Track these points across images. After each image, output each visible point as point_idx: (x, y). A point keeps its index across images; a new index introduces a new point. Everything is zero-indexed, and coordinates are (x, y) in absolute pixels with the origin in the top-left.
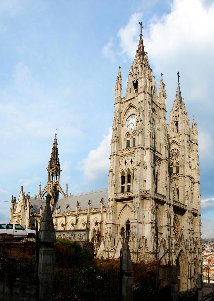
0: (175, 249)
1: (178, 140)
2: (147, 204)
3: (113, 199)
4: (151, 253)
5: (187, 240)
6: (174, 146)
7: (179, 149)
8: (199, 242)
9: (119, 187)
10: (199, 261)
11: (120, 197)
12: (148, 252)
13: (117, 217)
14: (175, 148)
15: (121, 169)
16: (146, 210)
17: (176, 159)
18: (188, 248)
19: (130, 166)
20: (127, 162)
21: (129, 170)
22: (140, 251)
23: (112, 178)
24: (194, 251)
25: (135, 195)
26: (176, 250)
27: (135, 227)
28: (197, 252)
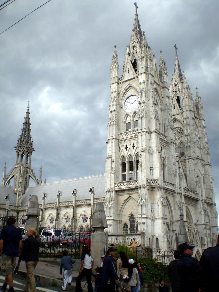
2: (156, 195)
6: (176, 124)
11: (121, 187)
14: (177, 126)
15: (122, 155)
19: (133, 152)
20: (128, 146)
21: (130, 155)
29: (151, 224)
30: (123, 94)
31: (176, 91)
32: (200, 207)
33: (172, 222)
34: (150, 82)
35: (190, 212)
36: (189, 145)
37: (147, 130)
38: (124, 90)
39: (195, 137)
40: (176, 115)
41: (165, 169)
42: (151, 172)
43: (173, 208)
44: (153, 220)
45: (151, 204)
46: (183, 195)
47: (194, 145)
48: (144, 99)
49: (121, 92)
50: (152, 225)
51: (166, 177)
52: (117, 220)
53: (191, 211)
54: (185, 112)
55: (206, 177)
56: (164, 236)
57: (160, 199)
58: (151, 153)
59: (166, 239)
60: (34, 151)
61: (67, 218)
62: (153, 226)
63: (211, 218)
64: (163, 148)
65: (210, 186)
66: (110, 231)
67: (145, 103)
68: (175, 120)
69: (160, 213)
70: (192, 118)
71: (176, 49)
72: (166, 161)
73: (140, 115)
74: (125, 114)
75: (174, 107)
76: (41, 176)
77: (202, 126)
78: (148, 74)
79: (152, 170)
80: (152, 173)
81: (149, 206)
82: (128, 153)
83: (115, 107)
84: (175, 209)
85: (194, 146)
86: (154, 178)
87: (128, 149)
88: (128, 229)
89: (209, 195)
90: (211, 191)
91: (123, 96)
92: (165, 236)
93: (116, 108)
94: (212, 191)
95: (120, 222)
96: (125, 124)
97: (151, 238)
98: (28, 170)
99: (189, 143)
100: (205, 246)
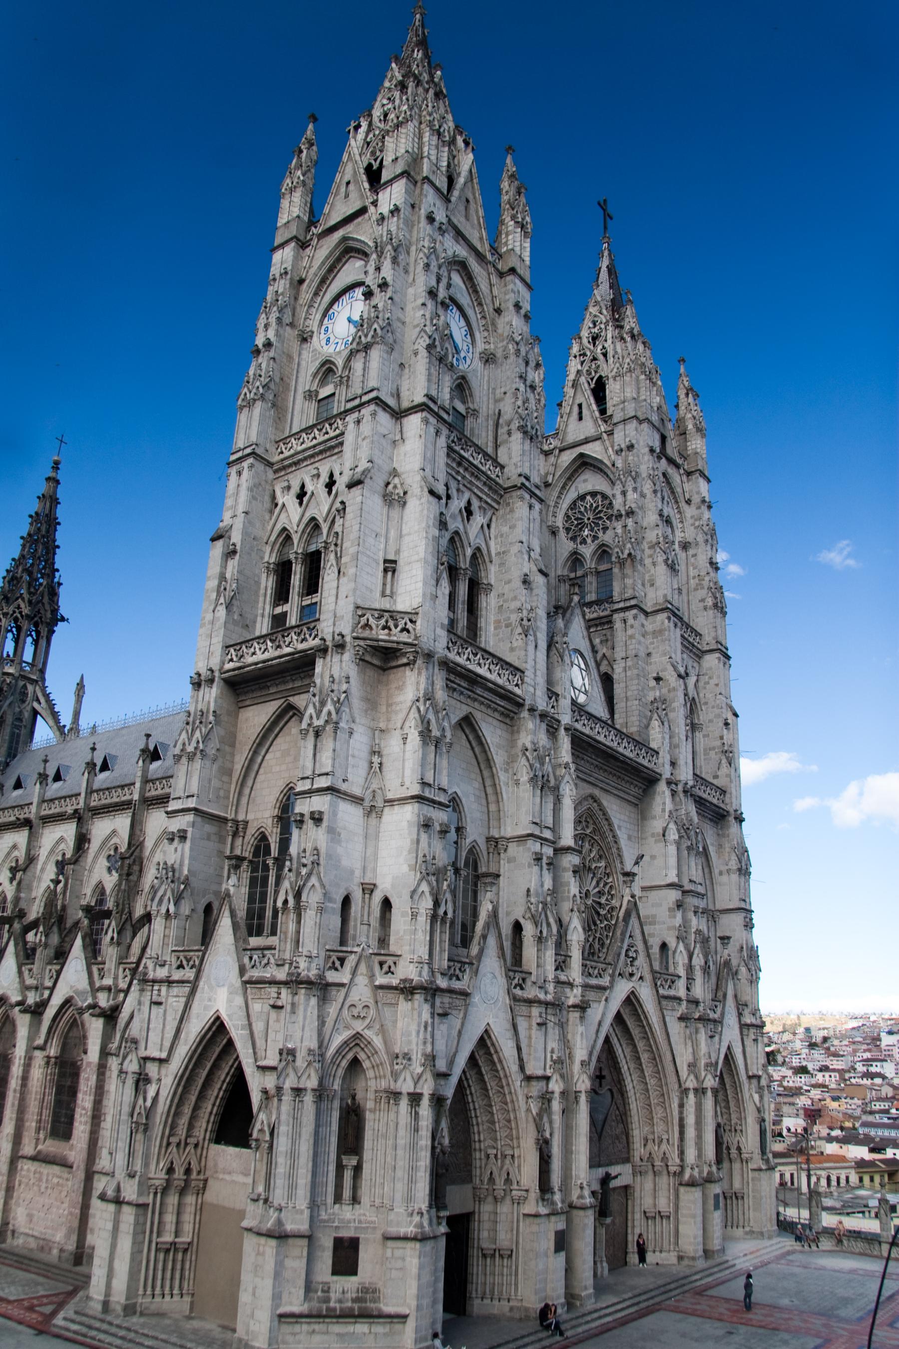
0: (586, 986)
1: (606, 450)
2: (400, 688)
3: (217, 674)
4: (408, 990)
5: (664, 946)
6: (585, 481)
7: (608, 492)
8: (743, 969)
9: (259, 619)
11: (250, 660)
12: (395, 982)
13: (234, 780)
15: (279, 527)
16: (390, 726)
17: (595, 538)
18: (672, 993)
19: (321, 507)
20: (309, 488)
22: (343, 976)
23: (224, 566)
24: (712, 1015)
25: (329, 638)
26: (591, 995)
27: (312, 818)
28: (731, 1020)
29: (360, 831)
30: (315, 284)
31: (595, 359)
32: (663, 810)
33: (495, 844)
35: (610, 825)
36: (630, 555)
37: (391, 402)
38: (320, 268)
39: (660, 523)
40: (587, 441)
41: (484, 604)
42: (384, 584)
43: (502, 777)
44: (373, 808)
45: (373, 730)
46: (566, 729)
47: (650, 556)
48: (387, 271)
52: (226, 820)
53: (616, 822)
54: (621, 426)
55: (706, 703)
56: (419, 885)
57: (414, 709)
59: (427, 903)
60: (63, 619)
61: (112, 853)
62: (371, 837)
64: (480, 507)
65: (722, 738)
66: (176, 866)
67: (390, 289)
68: (584, 463)
69: (408, 772)
70: (647, 450)
71: (607, 216)
72: (493, 569)
73: (363, 338)
74: (317, 364)
75: (580, 413)
76: (77, 715)
77: (696, 499)
78: (419, 184)
79: (390, 574)
80: (388, 586)
81: (356, 736)
82: (303, 516)
83: (271, 334)
84: (517, 783)
85: (650, 560)
86: (400, 607)
87: (305, 499)
88: (270, 862)
91: (316, 294)
92: (424, 887)
93: (277, 334)
94: (727, 758)
95: (239, 828)
96: (314, 405)
97: (357, 895)
98: (30, 688)
99: (629, 546)
100: (673, 982)
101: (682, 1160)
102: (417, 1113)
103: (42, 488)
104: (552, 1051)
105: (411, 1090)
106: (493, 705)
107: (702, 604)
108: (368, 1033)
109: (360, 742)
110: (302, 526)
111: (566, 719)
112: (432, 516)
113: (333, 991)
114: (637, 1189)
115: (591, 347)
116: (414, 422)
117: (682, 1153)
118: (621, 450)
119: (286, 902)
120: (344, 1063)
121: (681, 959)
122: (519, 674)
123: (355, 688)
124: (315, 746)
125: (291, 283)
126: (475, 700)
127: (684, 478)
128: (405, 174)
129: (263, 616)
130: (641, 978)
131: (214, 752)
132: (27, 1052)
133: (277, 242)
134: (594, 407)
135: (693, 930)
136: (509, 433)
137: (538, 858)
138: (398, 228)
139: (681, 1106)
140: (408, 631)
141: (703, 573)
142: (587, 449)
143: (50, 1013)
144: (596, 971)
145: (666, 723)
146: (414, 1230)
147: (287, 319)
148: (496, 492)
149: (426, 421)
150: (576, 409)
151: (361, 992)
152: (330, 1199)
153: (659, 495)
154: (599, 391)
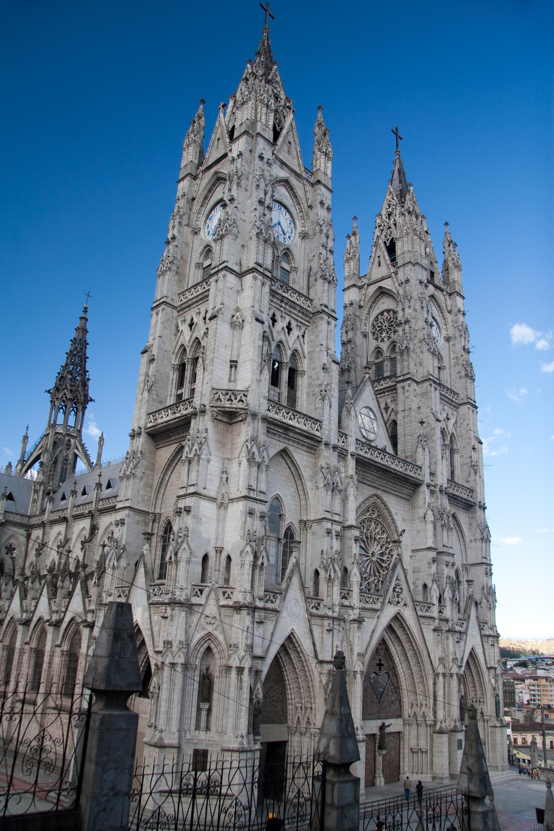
0: (363, 609)
1: (394, 283)
2: (238, 434)
3: (143, 430)
4: (238, 608)
5: (425, 586)
6: (383, 303)
8: (484, 601)
9: (169, 397)
10: (489, 668)
11: (160, 421)
12: (231, 603)
14: (386, 307)
15: (179, 344)
16: (233, 457)
17: (389, 338)
18: (428, 614)
20: (195, 320)
22: (201, 600)
24: (457, 628)
25: (198, 407)
27: (185, 510)
29: (215, 517)
30: (201, 200)
31: (390, 228)
32: (425, 503)
34: (257, 154)
36: (406, 347)
37: (236, 268)
39: (425, 326)
40: (383, 279)
42: (230, 375)
46: (352, 455)
47: (420, 347)
49: (198, 196)
50: (218, 520)
51: (299, 403)
52: (148, 513)
54: (402, 269)
56: (245, 547)
57: (245, 447)
58: (237, 325)
62: (221, 521)
63: (471, 541)
65: (471, 457)
68: (382, 292)
69: (241, 483)
70: (418, 282)
72: (306, 361)
74: (202, 247)
77: (455, 310)
79: (233, 368)
80: (233, 376)
83: (175, 232)
84: (317, 488)
85: (420, 350)
86: (239, 388)
89: (468, 482)
90: (472, 469)
91: (202, 206)
92: (248, 549)
93: (179, 232)
94: (474, 470)
96: (201, 271)
99: (406, 342)
101: (435, 717)
102: (241, 679)
103: (78, 323)
104: (337, 647)
105: (238, 665)
106: (301, 442)
107: (458, 375)
108: (215, 633)
109: (215, 466)
110: (191, 343)
111: (352, 448)
112: (258, 334)
113: (196, 608)
114: (407, 734)
115: (388, 220)
116: (249, 278)
117: (435, 713)
118: (402, 283)
119: (171, 558)
120: (202, 650)
121: (434, 594)
122: (318, 423)
123: (211, 435)
124: (189, 469)
125: (187, 201)
126: (289, 440)
127: (447, 297)
128: (246, 132)
129: (171, 395)
130: (405, 605)
131: (141, 474)
132: (51, 648)
133: (181, 176)
134: (387, 258)
135: (445, 576)
136: (316, 280)
137: (329, 532)
138: (242, 165)
139: (435, 684)
140: (243, 402)
141: (459, 356)
142: (383, 284)
143: (64, 625)
144: (371, 600)
145: (427, 450)
146: (238, 746)
147: (185, 222)
148: (307, 316)
149: (255, 278)
150: (377, 260)
151: (211, 609)
152: (193, 728)
153: (425, 309)
154: (391, 249)
